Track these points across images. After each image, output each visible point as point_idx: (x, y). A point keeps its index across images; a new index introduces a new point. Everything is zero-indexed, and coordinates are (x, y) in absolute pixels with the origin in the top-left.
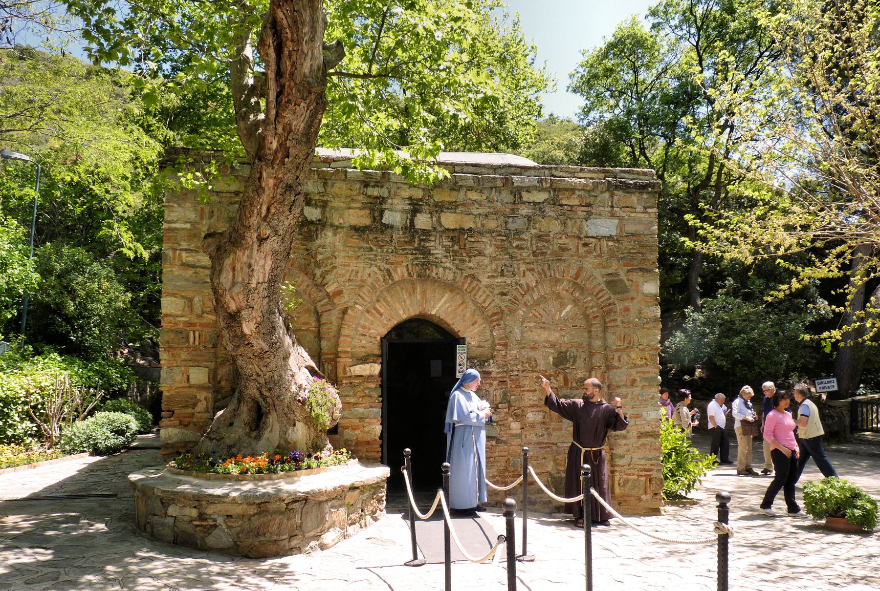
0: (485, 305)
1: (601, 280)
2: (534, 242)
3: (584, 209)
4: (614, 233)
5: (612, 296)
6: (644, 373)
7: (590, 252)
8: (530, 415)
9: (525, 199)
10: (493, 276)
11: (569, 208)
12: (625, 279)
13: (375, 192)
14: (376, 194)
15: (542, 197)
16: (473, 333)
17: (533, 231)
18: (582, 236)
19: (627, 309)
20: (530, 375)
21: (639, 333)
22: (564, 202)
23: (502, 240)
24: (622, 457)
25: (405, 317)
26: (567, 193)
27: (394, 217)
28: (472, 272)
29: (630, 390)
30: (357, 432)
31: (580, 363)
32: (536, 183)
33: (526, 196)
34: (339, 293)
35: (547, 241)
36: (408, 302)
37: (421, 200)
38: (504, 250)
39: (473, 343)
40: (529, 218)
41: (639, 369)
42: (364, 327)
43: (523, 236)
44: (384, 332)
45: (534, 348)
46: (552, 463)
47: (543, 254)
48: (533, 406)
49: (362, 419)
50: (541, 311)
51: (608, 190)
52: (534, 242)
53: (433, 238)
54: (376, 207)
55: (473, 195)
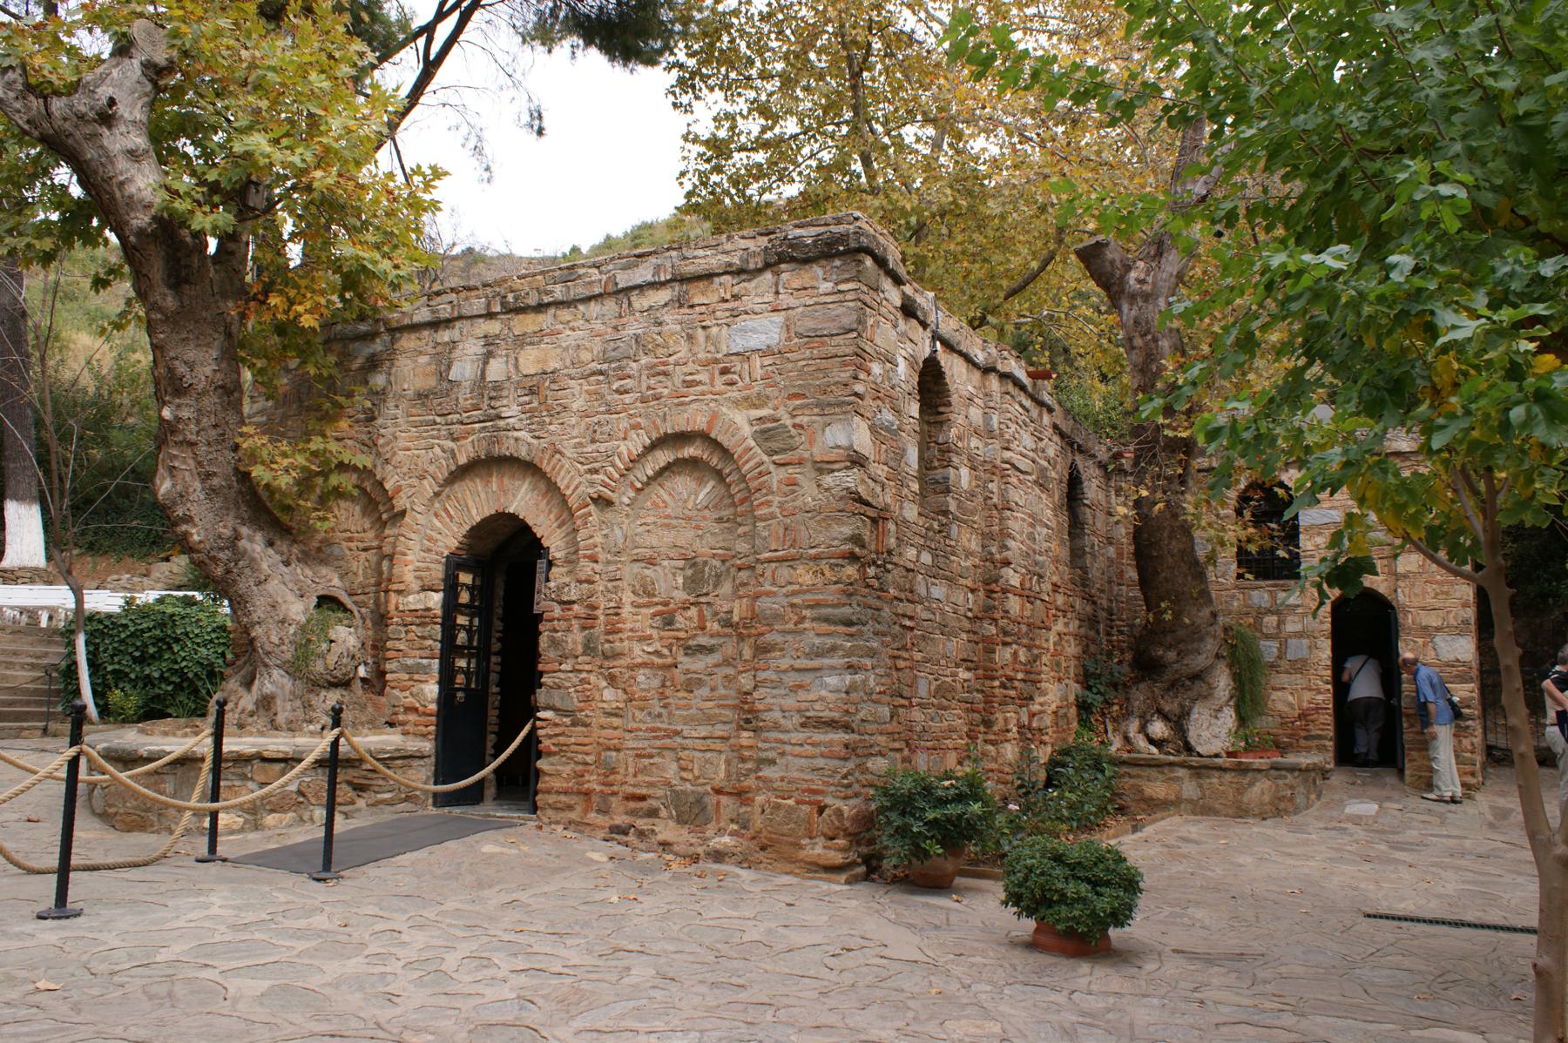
0: (568, 492)
1: (747, 430)
2: (644, 377)
3: (726, 306)
4: (773, 342)
5: (765, 458)
6: (818, 605)
7: (732, 384)
8: (641, 678)
9: (636, 305)
10: (580, 445)
11: (703, 309)
12: (789, 422)
13: (445, 336)
14: (446, 339)
15: (664, 295)
16: (554, 541)
17: (644, 360)
18: (719, 356)
19: (793, 483)
20: (643, 610)
21: (813, 524)
22: (696, 301)
23: (599, 382)
24: (772, 762)
25: (478, 519)
26: (701, 285)
27: (463, 369)
28: (554, 438)
29: (789, 638)
30: (407, 693)
31: (726, 588)
32: (649, 278)
33: (640, 302)
34: (398, 490)
35: (665, 374)
36: (483, 496)
37: (497, 336)
38: (599, 396)
39: (558, 555)
40: (637, 337)
41: (808, 597)
42: (430, 539)
43: (628, 371)
44: (453, 544)
45: (651, 562)
46: (674, 766)
47: (657, 398)
48: (644, 665)
49: (410, 670)
50: (666, 497)
51: (767, 266)
52: (644, 377)
53: (505, 393)
54: (444, 359)
55: (565, 314)
